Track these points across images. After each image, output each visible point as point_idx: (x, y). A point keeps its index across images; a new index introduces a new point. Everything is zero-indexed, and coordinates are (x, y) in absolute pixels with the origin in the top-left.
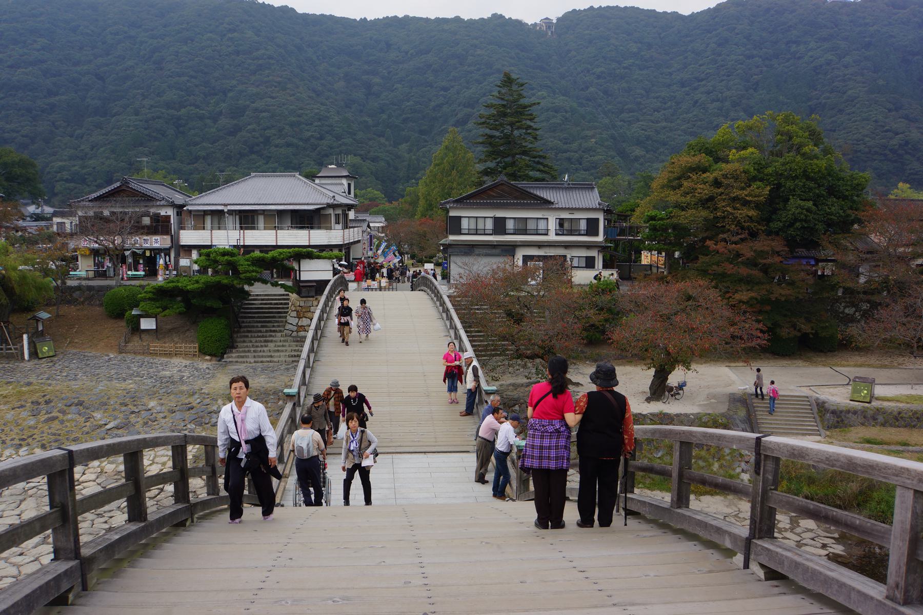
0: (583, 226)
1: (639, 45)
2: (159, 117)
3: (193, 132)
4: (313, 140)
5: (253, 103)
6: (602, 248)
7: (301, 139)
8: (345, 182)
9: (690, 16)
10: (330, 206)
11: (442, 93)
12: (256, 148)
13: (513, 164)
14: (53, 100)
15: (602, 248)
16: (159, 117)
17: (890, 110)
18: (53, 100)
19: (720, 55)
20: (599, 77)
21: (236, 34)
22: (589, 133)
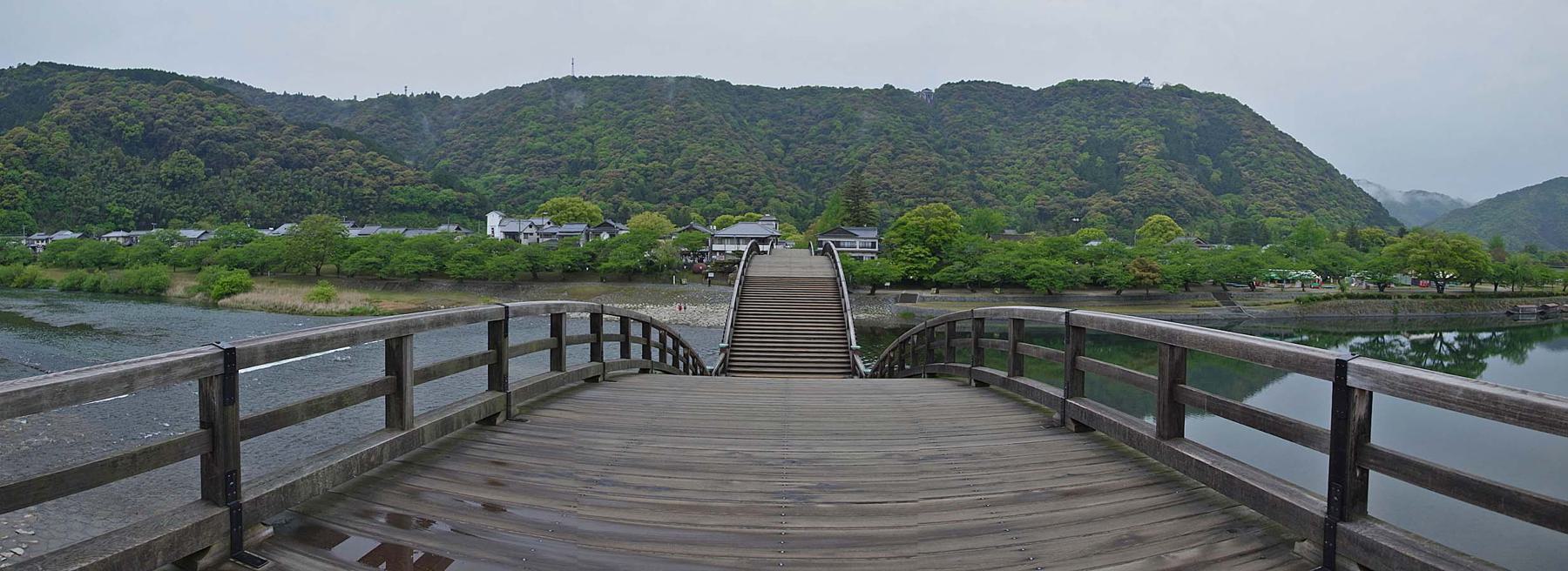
0: (870, 244)
1: (998, 113)
2: (633, 169)
3: (657, 180)
4: (744, 186)
5: (700, 157)
6: (877, 253)
7: (736, 185)
8: (774, 223)
9: (1038, 91)
10: (772, 236)
11: (844, 149)
12: (703, 192)
13: (858, 216)
14: (558, 159)
15: (877, 253)
16: (633, 169)
17: (1169, 171)
18: (558, 159)
19: (1057, 123)
20: (965, 138)
21: (686, 105)
22: (952, 182)
